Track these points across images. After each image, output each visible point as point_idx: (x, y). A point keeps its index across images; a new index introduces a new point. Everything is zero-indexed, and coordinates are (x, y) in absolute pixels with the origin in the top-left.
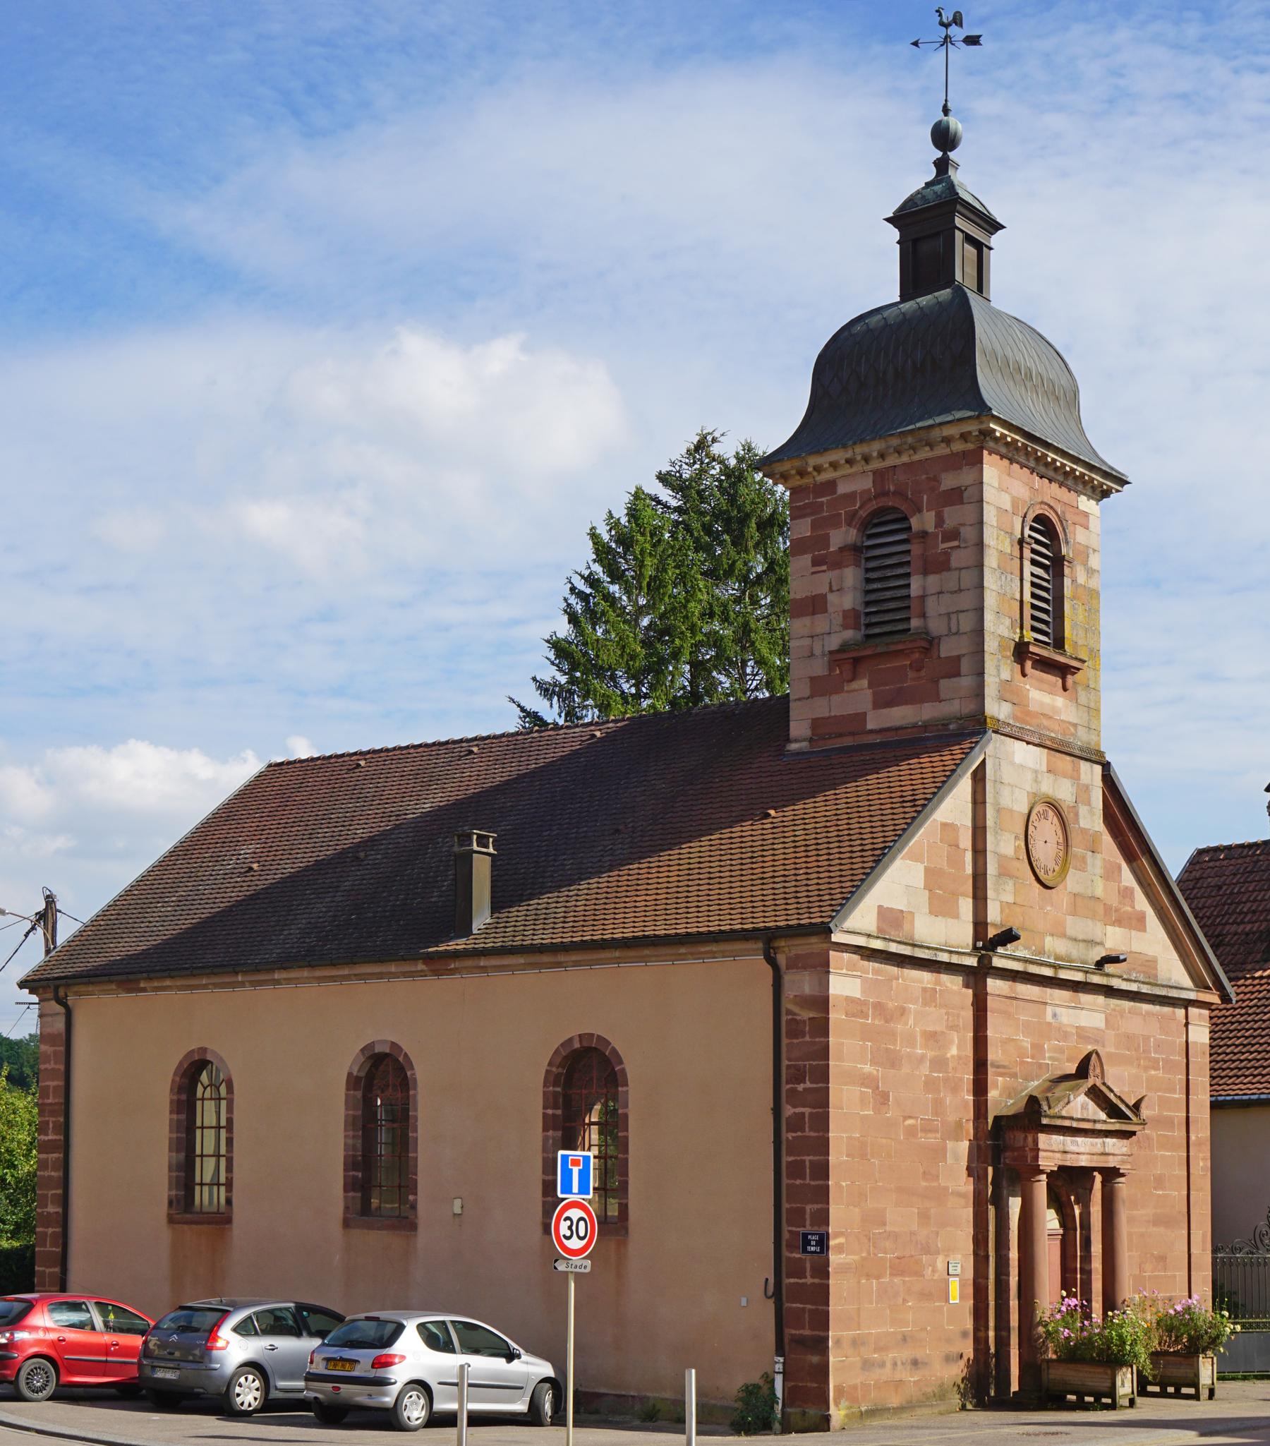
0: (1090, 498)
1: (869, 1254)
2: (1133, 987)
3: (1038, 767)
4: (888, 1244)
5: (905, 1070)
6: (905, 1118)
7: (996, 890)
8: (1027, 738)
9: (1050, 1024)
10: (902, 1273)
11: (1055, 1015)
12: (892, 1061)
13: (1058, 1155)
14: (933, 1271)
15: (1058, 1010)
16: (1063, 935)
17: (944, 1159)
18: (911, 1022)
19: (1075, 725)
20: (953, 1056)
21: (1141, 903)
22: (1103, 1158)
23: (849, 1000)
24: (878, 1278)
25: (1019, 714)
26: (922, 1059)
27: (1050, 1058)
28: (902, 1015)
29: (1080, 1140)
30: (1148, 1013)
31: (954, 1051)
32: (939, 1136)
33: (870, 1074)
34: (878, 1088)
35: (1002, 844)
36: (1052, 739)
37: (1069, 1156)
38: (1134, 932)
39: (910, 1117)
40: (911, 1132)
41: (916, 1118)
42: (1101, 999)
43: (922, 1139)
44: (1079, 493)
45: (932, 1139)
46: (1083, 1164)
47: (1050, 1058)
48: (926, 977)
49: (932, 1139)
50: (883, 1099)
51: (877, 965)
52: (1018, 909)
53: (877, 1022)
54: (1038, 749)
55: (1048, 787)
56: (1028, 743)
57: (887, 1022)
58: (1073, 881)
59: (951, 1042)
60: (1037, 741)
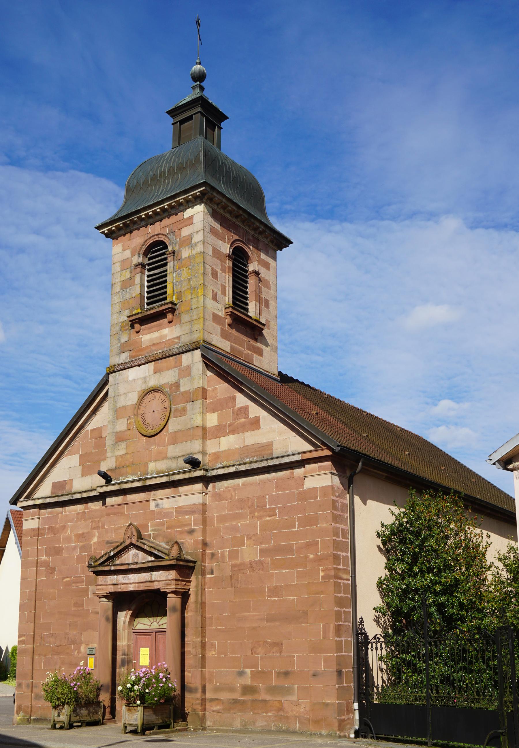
0: (192, 207)
1: (40, 644)
2: (232, 470)
3: (147, 374)
4: (52, 640)
5: (65, 554)
6: (64, 578)
7: (113, 451)
8: (138, 363)
9: (154, 511)
10: (58, 653)
11: (157, 505)
12: (58, 551)
13: (112, 587)
14: (78, 653)
15: (160, 502)
16: (166, 458)
17: (88, 595)
18: (69, 531)
19: (179, 338)
20: (94, 543)
21: (255, 411)
22: (148, 584)
23: (33, 530)
24: (45, 656)
25: (134, 354)
26: (75, 548)
27: (152, 531)
28: (64, 529)
29: (130, 576)
30: (262, 482)
31: (95, 540)
32: (84, 584)
33: (45, 560)
34: (49, 566)
35: (118, 427)
36: (152, 356)
37: (119, 586)
38: (247, 434)
39: (67, 577)
40: (68, 584)
41: (71, 577)
42: (199, 486)
43: (74, 586)
44: (183, 211)
45: (79, 586)
46: (132, 589)
47: (152, 531)
48: (79, 508)
49: (79, 586)
50: (52, 571)
51: (50, 510)
52: (128, 456)
53: (49, 536)
54: (147, 365)
55: (153, 382)
56: (139, 366)
57: (55, 534)
58: (173, 426)
59: (94, 535)
60: (143, 361)
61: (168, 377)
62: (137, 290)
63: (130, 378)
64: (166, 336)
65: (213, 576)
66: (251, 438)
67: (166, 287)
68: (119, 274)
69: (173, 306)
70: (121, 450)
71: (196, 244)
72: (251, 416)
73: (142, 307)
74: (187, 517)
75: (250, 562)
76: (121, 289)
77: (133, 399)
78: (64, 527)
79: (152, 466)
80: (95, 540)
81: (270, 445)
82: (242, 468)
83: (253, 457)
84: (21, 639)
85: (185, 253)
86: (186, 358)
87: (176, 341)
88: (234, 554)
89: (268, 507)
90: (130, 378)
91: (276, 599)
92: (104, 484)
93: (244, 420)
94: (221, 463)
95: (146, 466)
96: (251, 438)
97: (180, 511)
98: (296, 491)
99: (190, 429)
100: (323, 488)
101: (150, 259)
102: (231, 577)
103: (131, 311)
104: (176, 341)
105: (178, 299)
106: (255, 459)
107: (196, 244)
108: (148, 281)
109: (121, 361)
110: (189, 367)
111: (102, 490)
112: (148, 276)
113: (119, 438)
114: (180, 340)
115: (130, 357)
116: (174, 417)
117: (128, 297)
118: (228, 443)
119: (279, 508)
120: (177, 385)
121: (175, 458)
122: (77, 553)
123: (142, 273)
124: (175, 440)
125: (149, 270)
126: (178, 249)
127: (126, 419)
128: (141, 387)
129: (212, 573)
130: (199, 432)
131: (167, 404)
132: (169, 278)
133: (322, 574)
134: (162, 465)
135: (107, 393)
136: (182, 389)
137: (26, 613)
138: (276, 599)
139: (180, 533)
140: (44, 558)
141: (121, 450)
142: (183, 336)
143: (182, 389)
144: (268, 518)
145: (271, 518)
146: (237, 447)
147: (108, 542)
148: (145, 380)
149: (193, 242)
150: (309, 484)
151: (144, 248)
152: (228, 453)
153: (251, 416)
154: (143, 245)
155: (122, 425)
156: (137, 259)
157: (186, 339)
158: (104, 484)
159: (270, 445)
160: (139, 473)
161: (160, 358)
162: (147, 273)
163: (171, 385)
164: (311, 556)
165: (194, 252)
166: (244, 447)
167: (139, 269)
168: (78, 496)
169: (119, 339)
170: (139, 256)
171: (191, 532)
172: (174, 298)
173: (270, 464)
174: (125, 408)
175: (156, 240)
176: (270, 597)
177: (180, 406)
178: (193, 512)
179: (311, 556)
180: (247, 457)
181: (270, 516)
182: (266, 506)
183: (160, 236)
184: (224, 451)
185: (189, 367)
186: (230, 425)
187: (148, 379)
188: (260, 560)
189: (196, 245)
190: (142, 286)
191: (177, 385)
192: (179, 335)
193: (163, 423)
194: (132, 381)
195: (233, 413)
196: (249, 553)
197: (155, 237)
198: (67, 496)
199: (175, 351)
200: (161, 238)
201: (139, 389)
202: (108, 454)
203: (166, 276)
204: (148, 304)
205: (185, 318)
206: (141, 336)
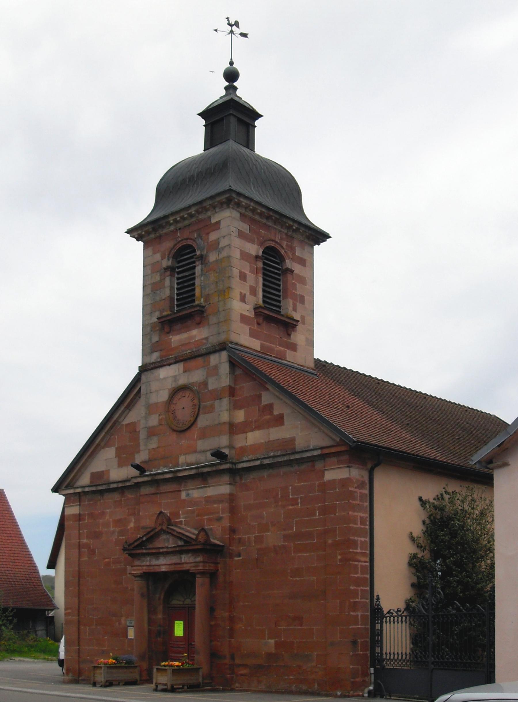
3: (177, 373)
6: (104, 559)
9: (184, 500)
11: (188, 495)
12: (97, 535)
14: (119, 624)
16: (195, 452)
18: (107, 517)
19: (207, 339)
20: (131, 528)
23: (74, 515)
26: (114, 532)
31: (132, 525)
32: (123, 564)
39: (107, 558)
40: (108, 564)
41: (110, 558)
47: (183, 518)
50: (92, 552)
55: (183, 381)
58: (203, 421)
61: (196, 376)
62: (167, 292)
63: (161, 377)
64: (195, 336)
65: (241, 558)
66: (276, 434)
67: (194, 290)
68: (150, 277)
69: (201, 309)
70: (154, 444)
71: (223, 248)
72: (276, 413)
73: (171, 308)
74: (215, 506)
75: (275, 546)
76: (152, 291)
77: (164, 396)
78: (103, 514)
79: (182, 459)
80: (132, 525)
81: (292, 440)
82: (266, 462)
83: (278, 450)
84: (68, 611)
85: (212, 257)
86: (214, 359)
87: (204, 341)
88: (259, 539)
89: (291, 497)
90: (161, 377)
91: (298, 579)
92: (139, 475)
93: (269, 416)
94: (247, 457)
95: (177, 459)
96: (276, 434)
97: (209, 500)
98: (317, 483)
99: (217, 425)
100: (341, 480)
101: (179, 262)
102: (257, 559)
103: (161, 312)
104: (204, 341)
105: (205, 301)
106: (279, 453)
107: (223, 248)
108: (178, 284)
109: (153, 360)
110: (216, 368)
111: (136, 481)
112: (178, 279)
113: (152, 432)
114: (208, 341)
115: (161, 357)
116: (202, 414)
117: (158, 298)
118: (253, 438)
119: (301, 498)
120: (205, 384)
121: (204, 451)
122: (114, 538)
123: (172, 275)
124: (204, 435)
125: (179, 273)
126: (205, 253)
127: (157, 415)
128: (170, 385)
129: (239, 555)
130: (227, 427)
131: (196, 401)
132: (197, 282)
133: (339, 557)
134: (191, 458)
135: (140, 390)
136: (210, 388)
137: (71, 589)
138: (298, 579)
139: (210, 520)
140: (85, 541)
141: (154, 444)
142: (211, 337)
143: (210, 388)
144: (291, 507)
145: (293, 507)
146: (262, 441)
147: (143, 528)
148: (175, 378)
149: (220, 246)
150: (329, 476)
151: (173, 252)
152: (255, 448)
153: (276, 413)
154: (172, 249)
155: (154, 421)
156: (166, 263)
157: (214, 340)
158: (139, 475)
159: (292, 440)
160: (171, 465)
161: (188, 358)
162: (176, 276)
163: (200, 383)
164: (330, 541)
165: (221, 256)
166: (269, 442)
167: (168, 273)
168: (115, 486)
169: (150, 339)
170: (169, 260)
171: (219, 519)
172: (202, 300)
173: (292, 458)
174: (156, 404)
175: (185, 244)
176: (291, 577)
177: (208, 403)
178: (221, 501)
179: (330, 541)
180: (272, 450)
181: (293, 505)
182: (289, 496)
183: (189, 241)
184: (251, 445)
185: (216, 368)
186: (255, 422)
187: (178, 377)
188: (283, 545)
189: (223, 250)
190: (172, 288)
191: (205, 384)
192: (206, 336)
193: (192, 419)
194: (163, 379)
195: (259, 410)
196: (273, 538)
197: (184, 241)
198: (104, 486)
199: (203, 351)
200: (190, 242)
201: (169, 387)
202: (142, 447)
203: (194, 279)
204: (178, 306)
205: (213, 320)
206: (171, 337)
